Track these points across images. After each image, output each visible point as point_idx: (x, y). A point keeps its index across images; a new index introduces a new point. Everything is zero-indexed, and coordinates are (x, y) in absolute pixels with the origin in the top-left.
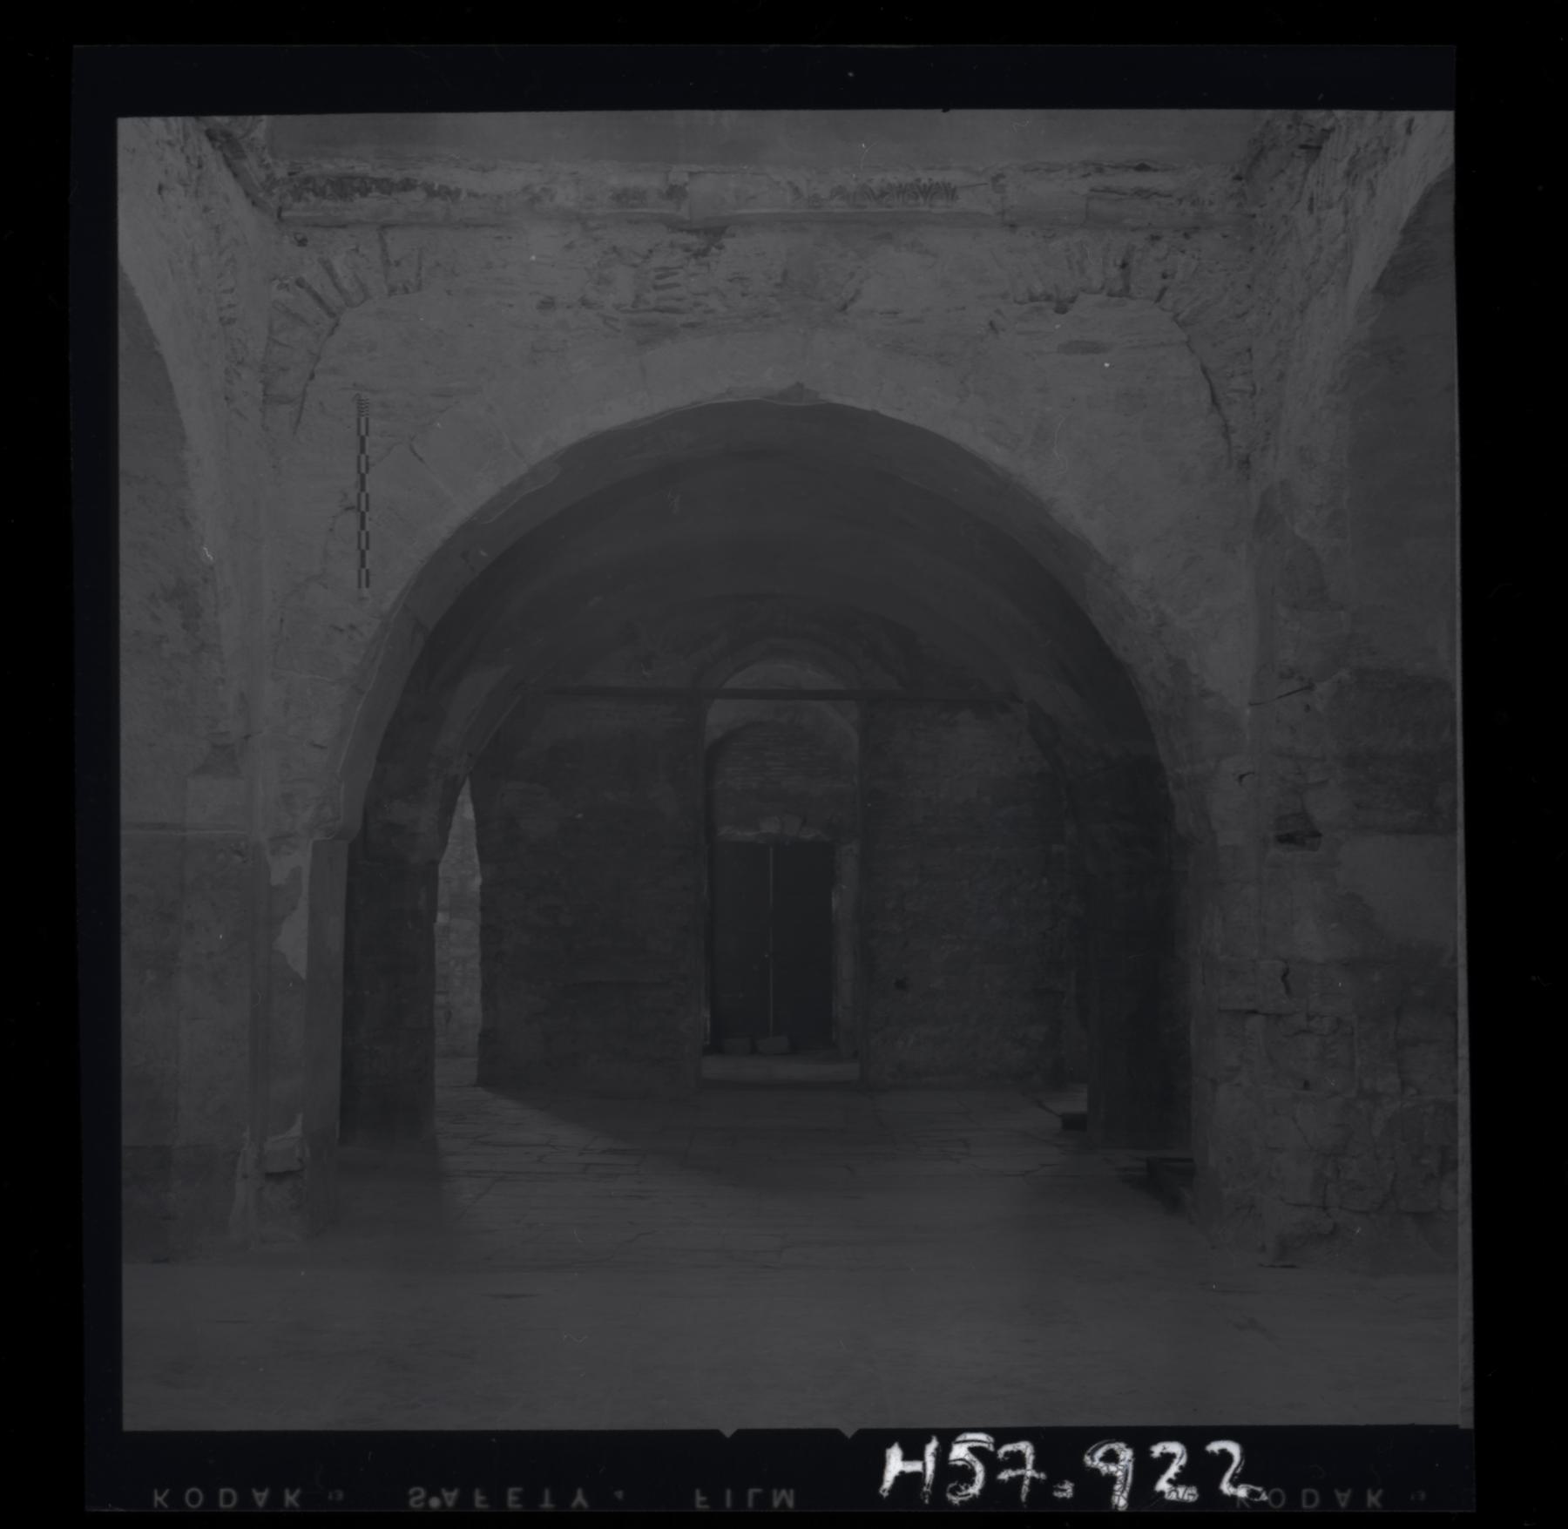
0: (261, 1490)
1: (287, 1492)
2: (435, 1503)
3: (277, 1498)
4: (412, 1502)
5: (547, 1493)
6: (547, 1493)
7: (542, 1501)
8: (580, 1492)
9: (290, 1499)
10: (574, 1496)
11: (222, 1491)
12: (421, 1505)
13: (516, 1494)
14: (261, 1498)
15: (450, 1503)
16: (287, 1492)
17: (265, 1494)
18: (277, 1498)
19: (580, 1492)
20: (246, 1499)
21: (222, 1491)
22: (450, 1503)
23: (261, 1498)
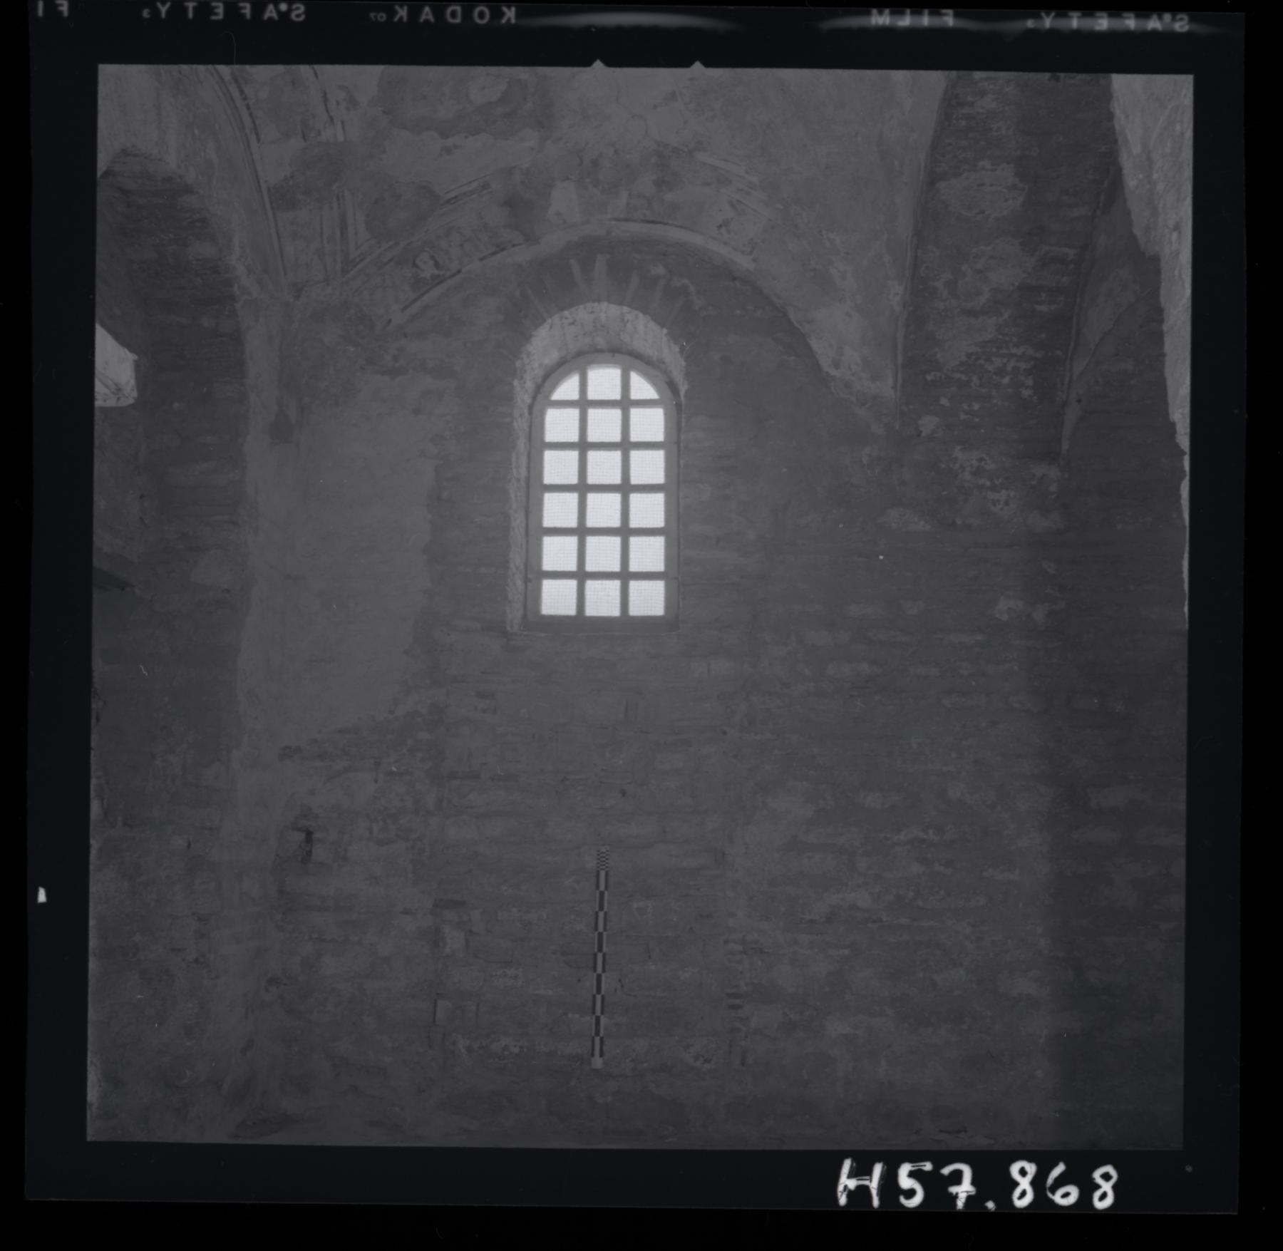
0: (427, 21)
1: (405, 19)
2: (283, 7)
3: (415, 13)
4: (302, 8)
5: (191, 15)
6: (191, 15)
7: (195, 8)
8: (163, 15)
9: (402, 13)
10: (168, 12)
11: (458, 20)
12: (294, 6)
13: (217, 14)
14: (427, 14)
15: (271, 7)
16: (405, 19)
17: (423, 18)
18: (415, 13)
19: (163, 15)
20: (439, 13)
21: (458, 20)
22: (271, 7)
23: (427, 14)
